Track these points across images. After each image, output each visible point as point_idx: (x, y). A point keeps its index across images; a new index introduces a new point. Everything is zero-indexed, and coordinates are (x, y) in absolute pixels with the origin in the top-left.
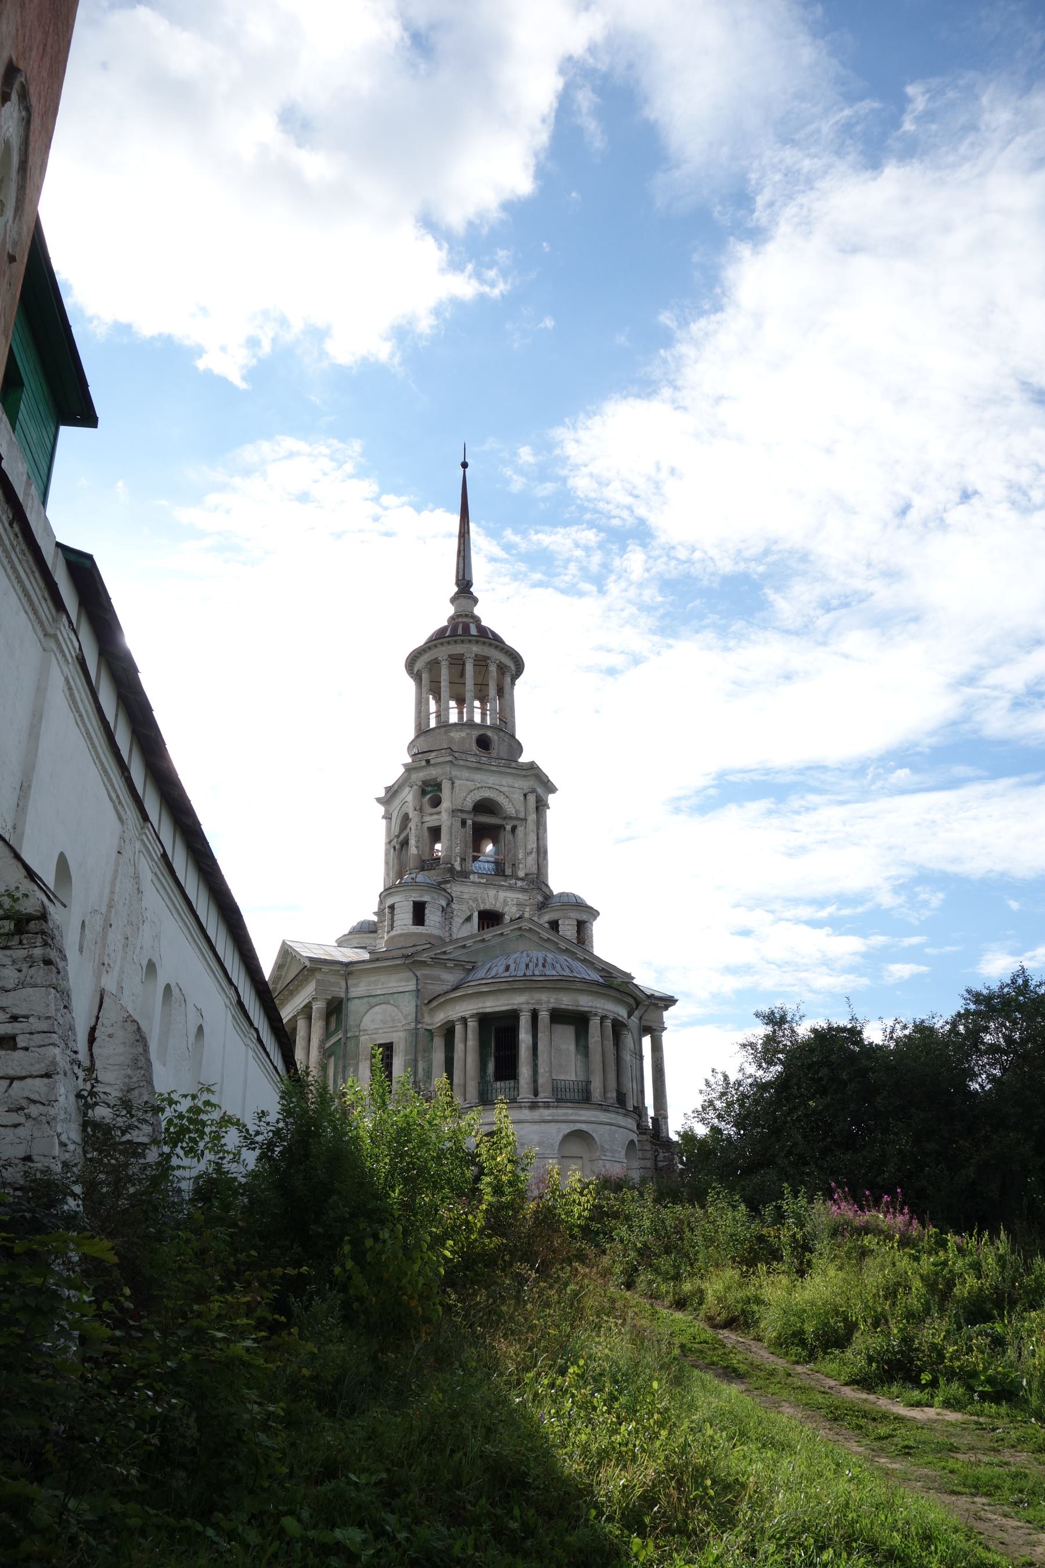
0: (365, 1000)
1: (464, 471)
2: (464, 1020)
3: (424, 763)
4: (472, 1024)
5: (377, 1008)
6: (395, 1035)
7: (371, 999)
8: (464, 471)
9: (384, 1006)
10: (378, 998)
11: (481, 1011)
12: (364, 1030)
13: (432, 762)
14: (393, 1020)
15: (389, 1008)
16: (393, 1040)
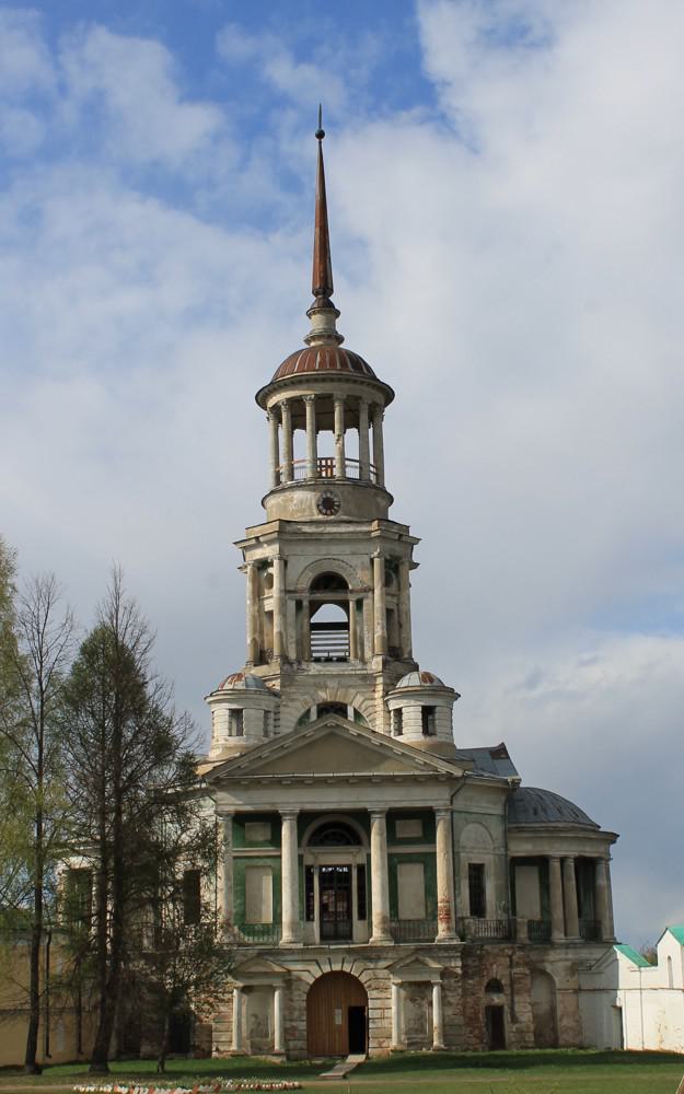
0: (463, 815)
1: (320, 143)
2: (563, 860)
3: (397, 537)
4: (571, 864)
5: (470, 826)
6: (487, 857)
7: (467, 815)
8: (320, 143)
9: (477, 825)
10: (473, 816)
11: (582, 854)
12: (464, 847)
13: (404, 538)
14: (484, 842)
15: (482, 829)
16: (486, 862)
